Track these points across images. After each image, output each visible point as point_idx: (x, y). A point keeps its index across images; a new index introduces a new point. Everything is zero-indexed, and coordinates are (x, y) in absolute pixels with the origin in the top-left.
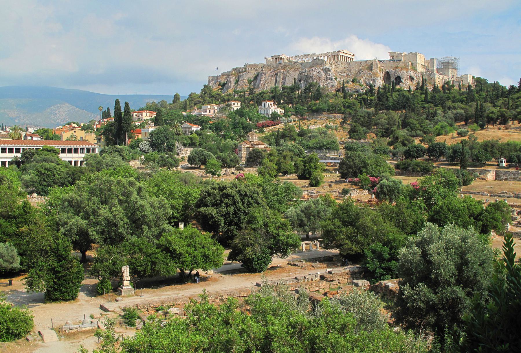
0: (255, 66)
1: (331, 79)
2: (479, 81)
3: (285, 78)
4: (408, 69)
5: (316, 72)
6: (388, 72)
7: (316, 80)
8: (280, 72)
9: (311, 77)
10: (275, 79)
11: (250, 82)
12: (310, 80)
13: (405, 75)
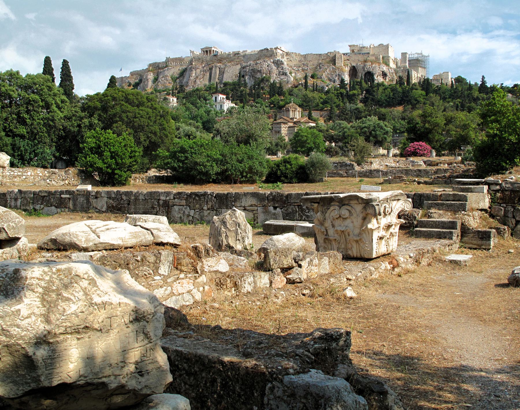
0: (180, 60)
1: (285, 74)
2: (459, 80)
3: (222, 73)
4: (379, 63)
5: (265, 66)
6: (354, 67)
7: (266, 74)
8: (216, 67)
9: (260, 71)
10: (208, 74)
11: (174, 80)
12: (258, 76)
13: (377, 70)
